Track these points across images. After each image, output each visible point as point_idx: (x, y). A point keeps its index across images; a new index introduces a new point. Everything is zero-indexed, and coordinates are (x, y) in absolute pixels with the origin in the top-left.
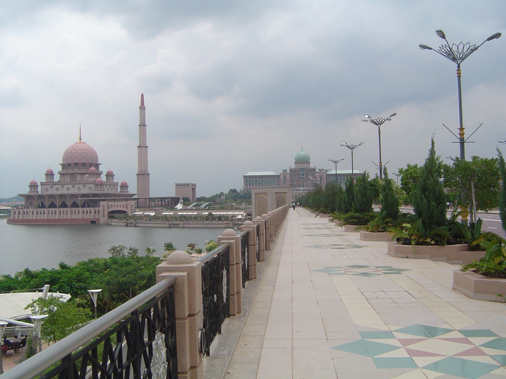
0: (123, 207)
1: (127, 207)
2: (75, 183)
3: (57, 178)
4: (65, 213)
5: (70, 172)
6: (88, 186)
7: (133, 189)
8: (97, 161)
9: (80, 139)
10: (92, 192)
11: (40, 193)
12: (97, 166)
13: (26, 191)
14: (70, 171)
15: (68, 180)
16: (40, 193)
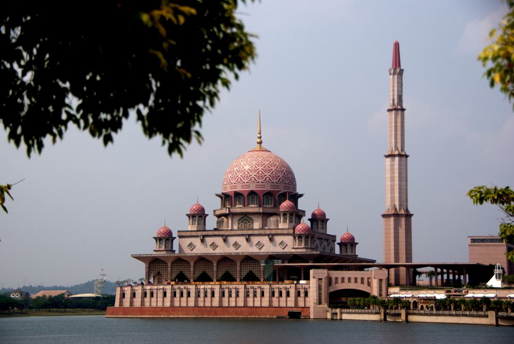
0: (362, 282)
1: (369, 284)
2: (250, 232)
3: (211, 223)
4: (234, 295)
5: (238, 210)
6: (278, 239)
7: (374, 245)
8: (295, 188)
9: (260, 143)
10: (289, 250)
11: (177, 252)
12: (295, 197)
13: (151, 248)
14: (239, 208)
15: (235, 227)
16: (177, 252)
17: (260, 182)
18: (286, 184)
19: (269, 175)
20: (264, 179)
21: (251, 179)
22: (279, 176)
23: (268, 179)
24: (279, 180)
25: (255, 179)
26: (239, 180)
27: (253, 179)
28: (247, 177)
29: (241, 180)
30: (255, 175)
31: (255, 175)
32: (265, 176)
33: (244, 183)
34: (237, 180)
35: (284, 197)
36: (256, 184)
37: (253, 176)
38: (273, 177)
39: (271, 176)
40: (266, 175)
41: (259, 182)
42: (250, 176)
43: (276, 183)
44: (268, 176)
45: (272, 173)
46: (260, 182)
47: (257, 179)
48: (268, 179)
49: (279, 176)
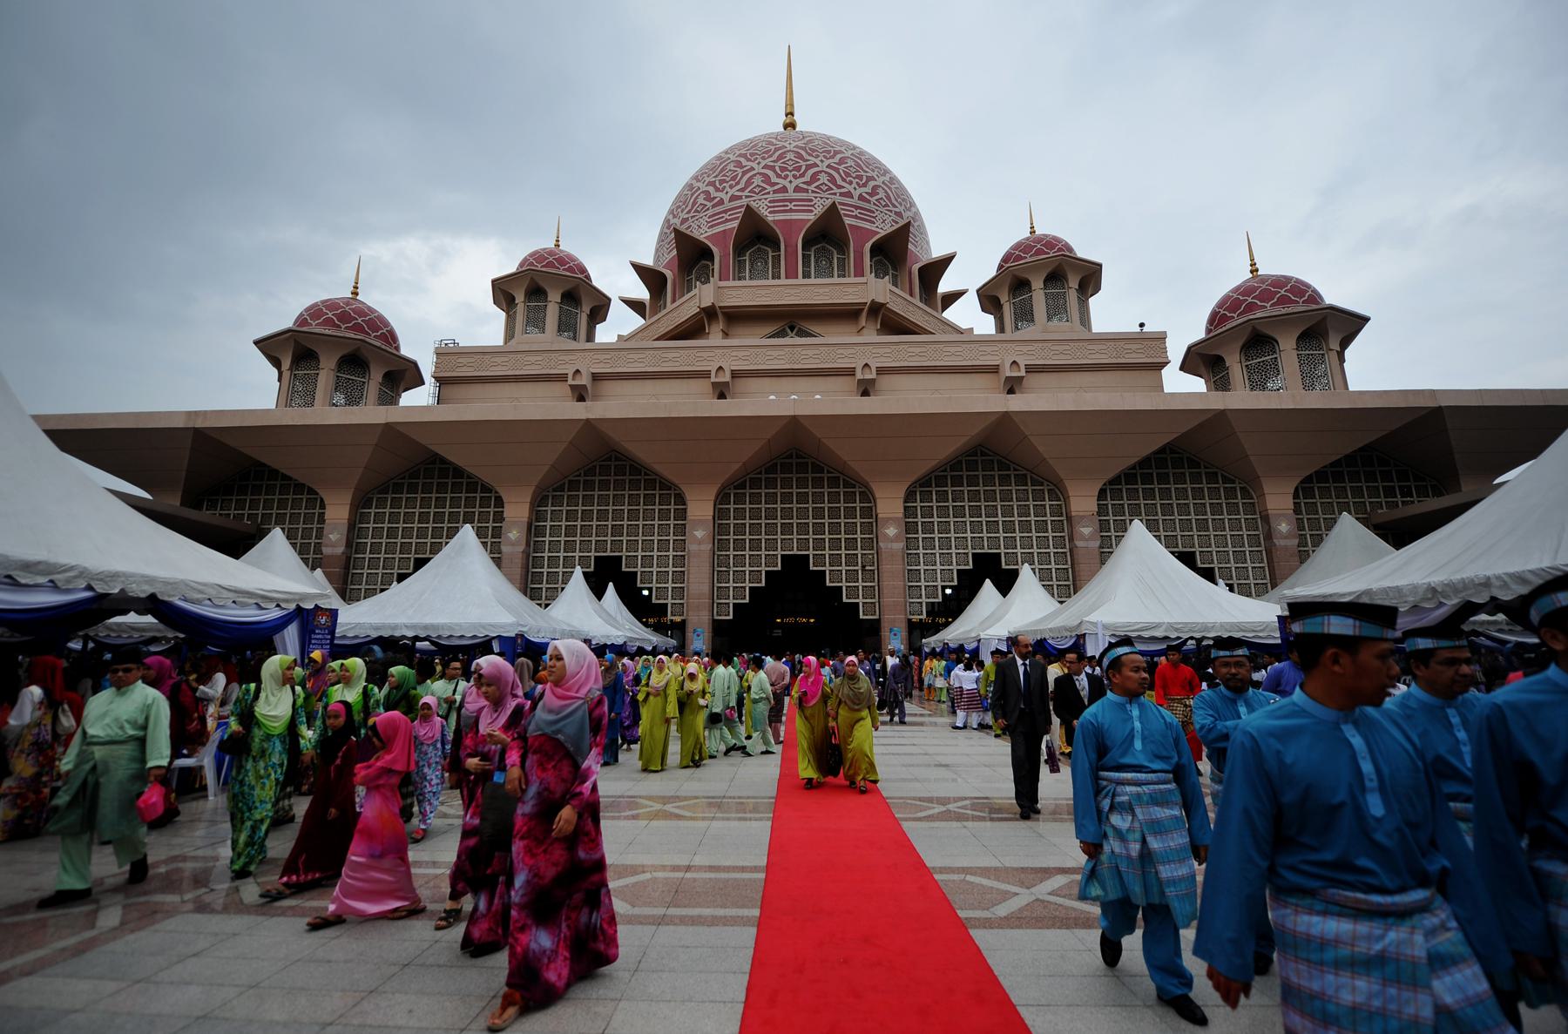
17: (791, 188)
18: (899, 214)
19: (829, 166)
20: (807, 178)
21: (749, 183)
22: (872, 178)
23: (823, 178)
24: (873, 193)
25: (767, 179)
26: (701, 200)
27: (758, 181)
28: (733, 179)
29: (709, 198)
30: (766, 167)
31: (766, 167)
32: (809, 167)
33: (721, 202)
34: (695, 203)
35: (895, 268)
36: (771, 197)
37: (758, 169)
38: (848, 175)
39: (837, 170)
40: (816, 165)
41: (784, 190)
42: (744, 173)
43: (861, 198)
44: (823, 167)
45: (842, 161)
46: (791, 188)
47: (774, 179)
48: (823, 178)
49: (872, 178)
